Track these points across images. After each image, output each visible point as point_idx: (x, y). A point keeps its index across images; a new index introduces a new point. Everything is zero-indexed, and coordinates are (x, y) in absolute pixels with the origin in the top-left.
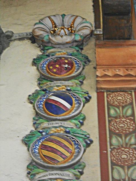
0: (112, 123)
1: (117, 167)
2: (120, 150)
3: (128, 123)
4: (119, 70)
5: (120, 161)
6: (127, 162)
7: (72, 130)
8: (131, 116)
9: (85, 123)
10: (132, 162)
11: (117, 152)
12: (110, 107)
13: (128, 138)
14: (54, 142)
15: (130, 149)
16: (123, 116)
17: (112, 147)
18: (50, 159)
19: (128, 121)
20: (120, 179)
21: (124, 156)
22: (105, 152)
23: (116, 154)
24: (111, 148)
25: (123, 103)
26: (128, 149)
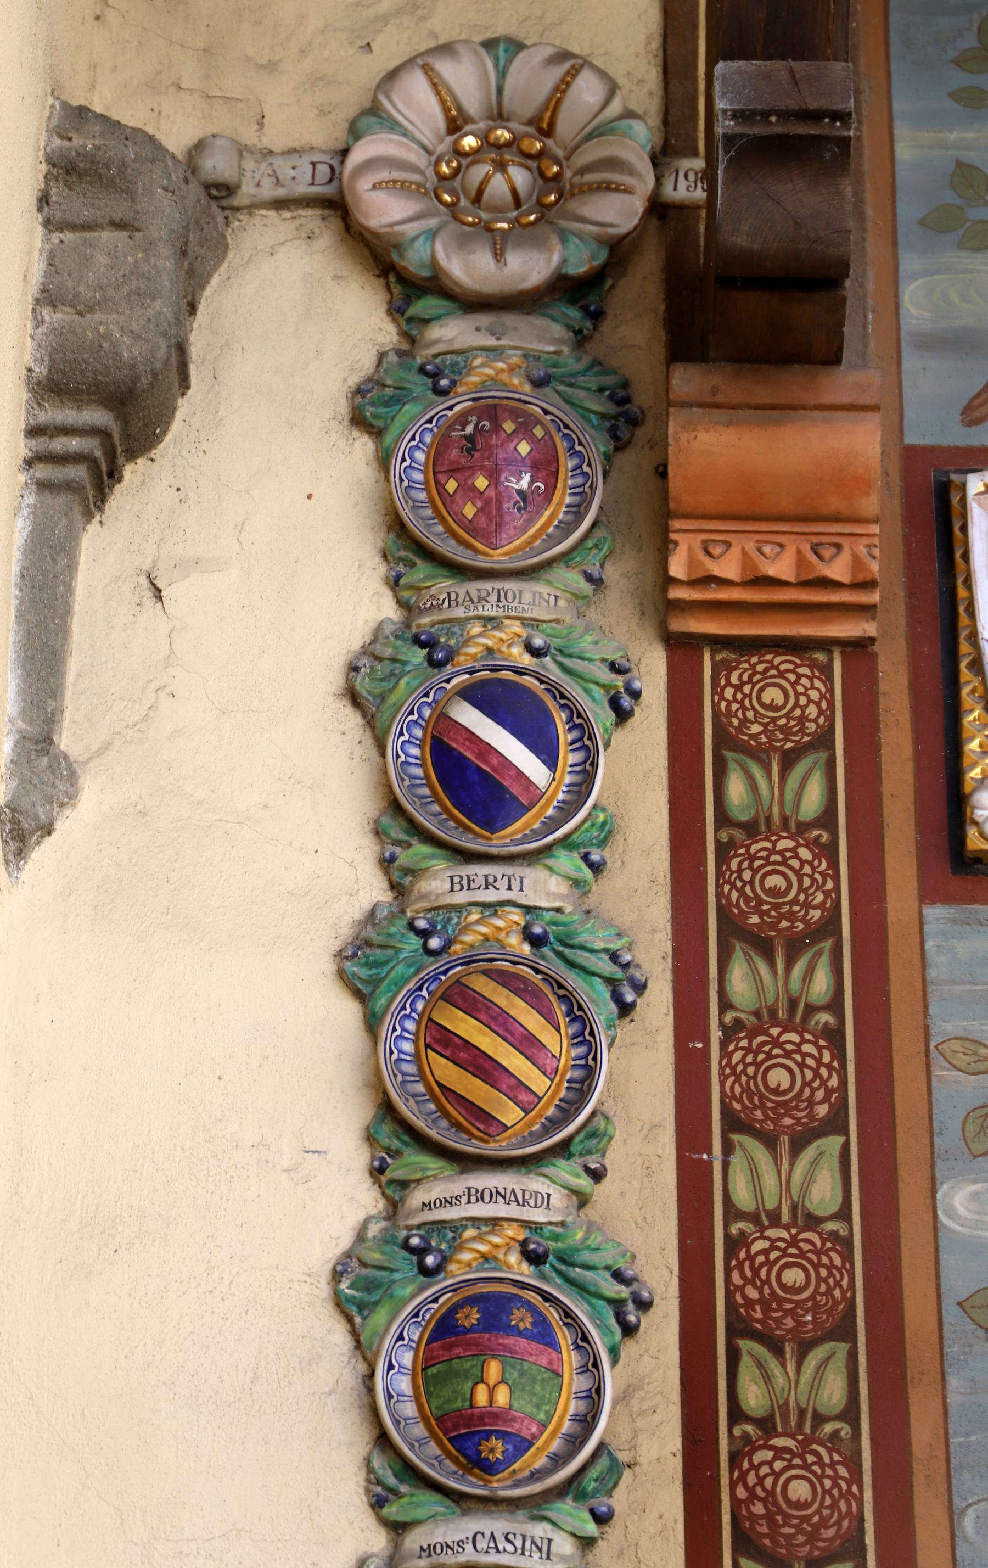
2: (761, 1038)
3: (802, 867)
4: (781, 546)
5: (763, 1107)
6: (785, 1115)
10: (811, 1116)
11: (748, 1050)
12: (728, 754)
13: (799, 968)
14: (482, 1017)
15: (807, 1036)
16: (785, 820)
17: (728, 1018)
18: (467, 1109)
19: (805, 853)
20: (757, 1208)
21: (779, 1078)
22: (700, 1045)
23: (743, 1060)
24: (722, 1024)
25: (785, 730)
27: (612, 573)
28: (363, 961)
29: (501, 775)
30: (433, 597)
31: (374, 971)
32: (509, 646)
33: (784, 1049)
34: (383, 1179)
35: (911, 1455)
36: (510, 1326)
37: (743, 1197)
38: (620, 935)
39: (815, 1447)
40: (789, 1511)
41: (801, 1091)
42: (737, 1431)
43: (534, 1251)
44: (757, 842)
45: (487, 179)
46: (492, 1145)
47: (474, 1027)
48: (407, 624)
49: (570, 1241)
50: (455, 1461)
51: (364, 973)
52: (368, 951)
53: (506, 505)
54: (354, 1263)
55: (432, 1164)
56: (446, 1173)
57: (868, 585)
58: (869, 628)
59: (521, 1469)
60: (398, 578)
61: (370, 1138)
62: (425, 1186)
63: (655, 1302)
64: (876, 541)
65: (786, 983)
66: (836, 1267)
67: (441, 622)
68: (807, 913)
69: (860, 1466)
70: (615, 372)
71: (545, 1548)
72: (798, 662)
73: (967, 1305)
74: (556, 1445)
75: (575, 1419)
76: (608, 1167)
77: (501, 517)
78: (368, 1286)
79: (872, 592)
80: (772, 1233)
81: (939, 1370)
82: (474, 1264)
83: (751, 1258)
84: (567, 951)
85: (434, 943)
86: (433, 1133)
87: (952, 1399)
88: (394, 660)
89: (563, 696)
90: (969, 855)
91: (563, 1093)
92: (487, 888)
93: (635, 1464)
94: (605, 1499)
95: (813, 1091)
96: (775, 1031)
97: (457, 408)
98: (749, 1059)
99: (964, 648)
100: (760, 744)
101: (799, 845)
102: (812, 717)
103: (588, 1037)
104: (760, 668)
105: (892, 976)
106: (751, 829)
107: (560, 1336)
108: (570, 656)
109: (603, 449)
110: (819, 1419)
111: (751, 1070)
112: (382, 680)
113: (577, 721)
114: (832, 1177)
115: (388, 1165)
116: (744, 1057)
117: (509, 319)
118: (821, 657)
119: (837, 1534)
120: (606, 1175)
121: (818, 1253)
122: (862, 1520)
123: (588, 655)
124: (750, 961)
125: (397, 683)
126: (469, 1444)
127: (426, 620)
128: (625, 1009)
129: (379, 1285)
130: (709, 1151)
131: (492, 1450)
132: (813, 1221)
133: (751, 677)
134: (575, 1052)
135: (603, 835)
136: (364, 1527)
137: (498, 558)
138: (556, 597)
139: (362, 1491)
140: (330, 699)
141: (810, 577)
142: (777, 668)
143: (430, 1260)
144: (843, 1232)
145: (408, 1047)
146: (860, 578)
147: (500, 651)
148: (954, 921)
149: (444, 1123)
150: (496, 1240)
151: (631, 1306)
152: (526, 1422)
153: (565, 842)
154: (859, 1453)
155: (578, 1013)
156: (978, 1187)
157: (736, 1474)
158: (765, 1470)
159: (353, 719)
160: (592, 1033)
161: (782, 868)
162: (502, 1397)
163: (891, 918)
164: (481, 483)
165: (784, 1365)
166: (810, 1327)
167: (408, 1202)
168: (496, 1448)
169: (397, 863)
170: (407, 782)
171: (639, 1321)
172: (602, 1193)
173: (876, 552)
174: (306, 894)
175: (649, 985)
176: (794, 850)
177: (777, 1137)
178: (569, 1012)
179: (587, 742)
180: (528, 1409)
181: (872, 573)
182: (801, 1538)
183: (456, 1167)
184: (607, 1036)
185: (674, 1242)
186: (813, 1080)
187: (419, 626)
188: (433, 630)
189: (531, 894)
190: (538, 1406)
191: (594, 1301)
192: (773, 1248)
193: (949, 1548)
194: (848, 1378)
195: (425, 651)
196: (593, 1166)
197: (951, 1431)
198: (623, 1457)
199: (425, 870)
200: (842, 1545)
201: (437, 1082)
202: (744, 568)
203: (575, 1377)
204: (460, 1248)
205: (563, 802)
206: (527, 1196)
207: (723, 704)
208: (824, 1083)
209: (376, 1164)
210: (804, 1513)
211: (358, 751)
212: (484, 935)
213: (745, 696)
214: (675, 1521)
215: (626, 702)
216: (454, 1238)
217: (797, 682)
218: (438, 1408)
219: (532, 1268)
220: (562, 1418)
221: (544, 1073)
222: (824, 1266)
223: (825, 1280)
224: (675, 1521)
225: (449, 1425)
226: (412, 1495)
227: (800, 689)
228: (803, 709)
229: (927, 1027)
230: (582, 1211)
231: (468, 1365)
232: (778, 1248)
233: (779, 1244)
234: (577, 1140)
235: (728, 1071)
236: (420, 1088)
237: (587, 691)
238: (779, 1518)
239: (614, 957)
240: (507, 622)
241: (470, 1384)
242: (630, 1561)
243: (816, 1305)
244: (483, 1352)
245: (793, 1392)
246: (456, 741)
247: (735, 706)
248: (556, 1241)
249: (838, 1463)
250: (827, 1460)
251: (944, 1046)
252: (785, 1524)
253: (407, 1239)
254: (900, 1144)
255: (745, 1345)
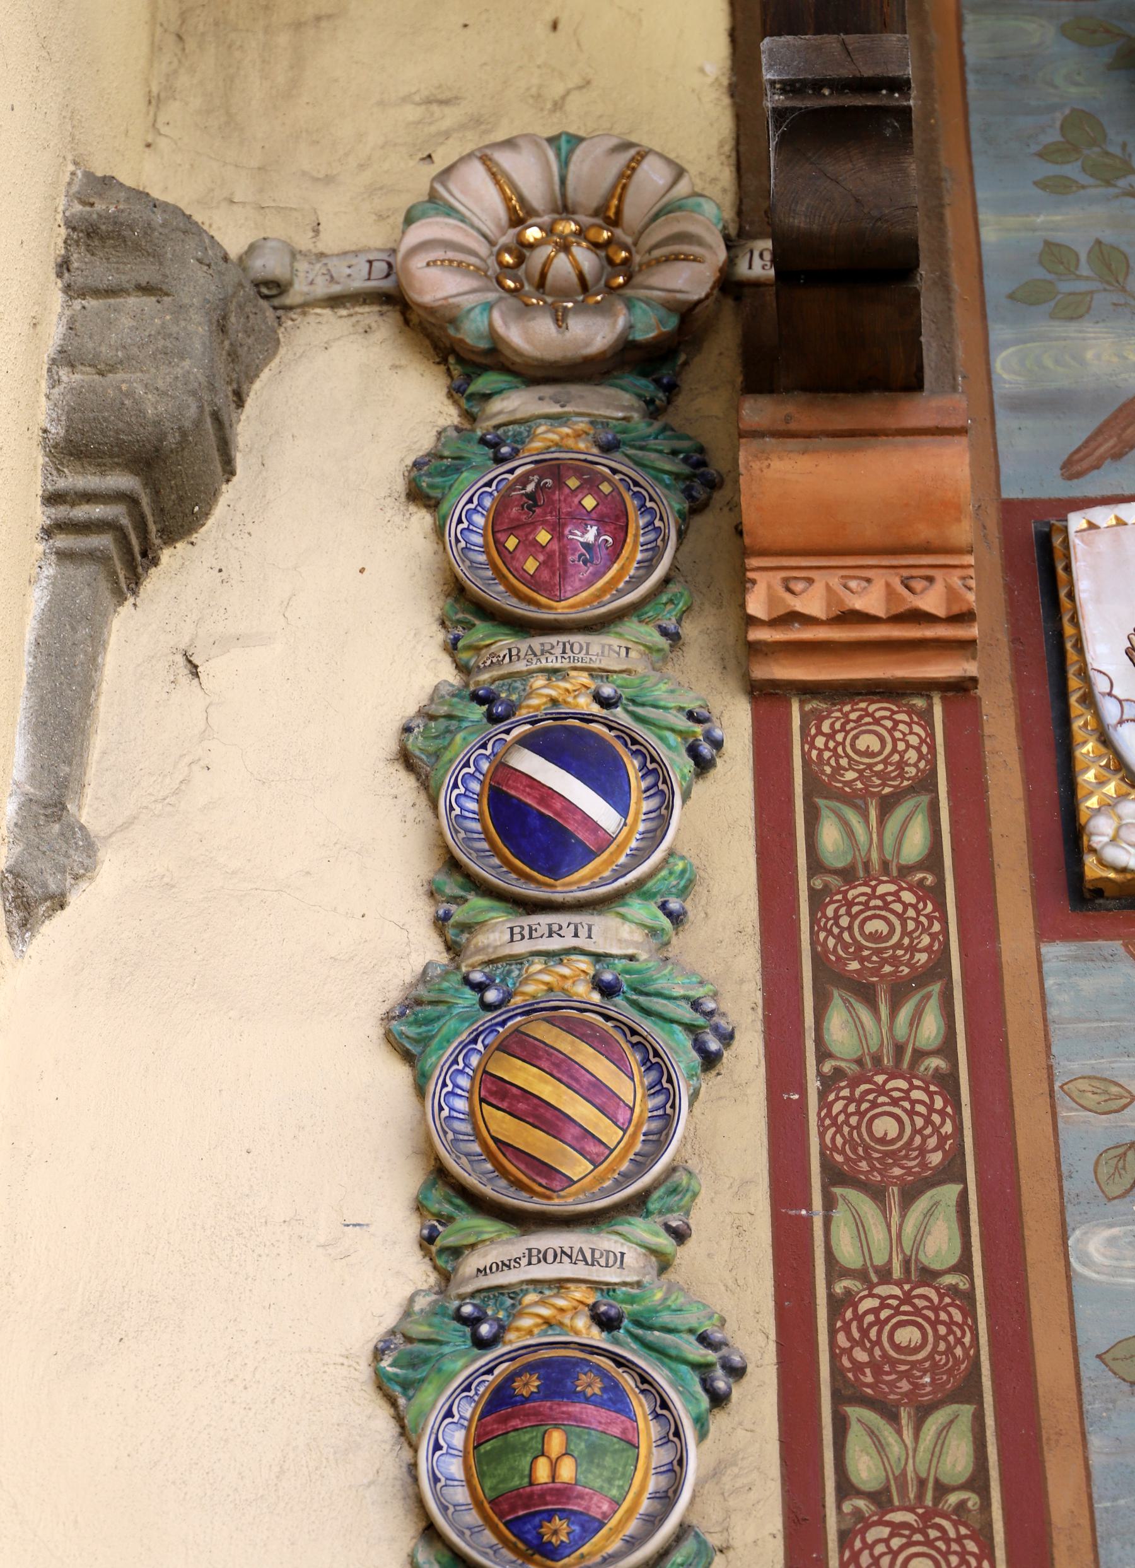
0: (830, 911)
1: (852, 1194)
3: (905, 910)
4: (868, 580)
5: (868, 1157)
6: (894, 1164)
7: (627, 972)
8: (920, 866)
9: (694, 909)
10: (924, 1165)
11: (850, 1100)
12: (821, 802)
13: (905, 1013)
14: (543, 1065)
15: (916, 1082)
16: (885, 865)
17: (827, 1068)
18: (527, 1164)
19: (908, 897)
20: (865, 1265)
21: (885, 1126)
22: (796, 1097)
23: (844, 1110)
24: (819, 1073)
25: (883, 776)
26: (904, 1078)
27: (689, 630)
28: (411, 1019)
29: (565, 820)
30: (493, 655)
31: (424, 1029)
32: (575, 697)
33: (890, 1097)
34: (434, 1249)
35: (1050, 1524)
36: (575, 1392)
37: (848, 1252)
38: (701, 983)
39: (938, 1520)
41: (911, 1139)
42: (847, 1507)
43: (604, 1313)
44: (855, 887)
45: (548, 261)
46: (556, 1201)
47: (534, 1076)
48: (467, 685)
49: (648, 1303)
50: (514, 1549)
51: (412, 1031)
52: (418, 1008)
53: (570, 558)
54: (399, 1340)
55: (488, 1227)
56: (505, 1237)
57: (964, 617)
58: (970, 668)
59: (591, 1554)
60: (457, 639)
61: (420, 1207)
62: (481, 1250)
63: (749, 1370)
64: (971, 572)
65: (891, 1029)
66: (957, 1324)
67: (502, 678)
68: (912, 957)
69: (992, 1539)
70: (689, 438)
72: (895, 708)
73: (1107, 1357)
74: (632, 1527)
75: (655, 1497)
76: (693, 1227)
77: (565, 571)
78: (414, 1362)
79: (970, 627)
80: (882, 1290)
81: (1078, 1429)
82: (536, 1331)
83: (859, 1318)
84: (642, 999)
85: (492, 996)
86: (488, 1190)
87: (1095, 1460)
88: (449, 717)
89: (635, 742)
90: (1088, 886)
91: (638, 1147)
92: (550, 936)
93: (728, 1548)
95: (925, 1139)
96: (880, 1079)
97: (518, 472)
98: (852, 1108)
99: (1074, 683)
100: (855, 790)
101: (901, 889)
102: (912, 761)
103: (666, 1085)
104: (853, 716)
105: (1009, 1016)
106: (848, 875)
107: (635, 1403)
108: (643, 705)
109: (677, 507)
110: (942, 1490)
111: (854, 1120)
112: (436, 737)
113: (651, 766)
114: (949, 1228)
115: (439, 1233)
116: (846, 1106)
117: (575, 389)
118: (920, 703)
120: (690, 1235)
121: (935, 1309)
123: (662, 703)
124: (850, 1008)
125: (452, 739)
126: (529, 1526)
127: (485, 677)
128: (710, 1060)
129: (426, 1360)
130: (808, 1206)
131: (555, 1532)
132: (928, 1276)
133: (843, 726)
134: (651, 1103)
135: (682, 883)
137: (561, 610)
138: (628, 649)
140: (382, 765)
141: (901, 609)
142: (872, 715)
143: (485, 1329)
144: (963, 1284)
145: (461, 1104)
146: (956, 610)
147: (565, 702)
148: (1076, 958)
149: (503, 1183)
150: (561, 1303)
151: (719, 1372)
152: (595, 1499)
153: (637, 887)
154: (989, 1525)
155: (654, 1060)
156: (1115, 1231)
157: (847, 1554)
158: (880, 1549)
159: (406, 783)
160: (670, 1080)
161: (883, 913)
162: (567, 1471)
163: (1006, 957)
164: (543, 537)
165: (899, 1432)
166: (928, 1389)
167: (461, 1271)
168: (560, 1530)
169: (452, 921)
170: (462, 835)
171: (730, 1389)
172: (686, 1255)
173: (972, 583)
174: (352, 959)
175: (737, 1035)
176: (896, 894)
177: (885, 1189)
178: (645, 1061)
179: (661, 786)
180: (598, 1483)
181: (968, 603)
183: (516, 1230)
184: (688, 1086)
185: (769, 1305)
186: (924, 1128)
187: (477, 683)
188: (493, 687)
189: (600, 941)
190: (610, 1481)
191: (674, 1365)
192: (883, 1306)
194: (974, 1443)
195: (485, 708)
196: (674, 1224)
197: (1095, 1496)
198: (714, 1540)
199: (482, 924)
201: (493, 1138)
202: (829, 605)
203: (654, 1450)
204: (521, 1314)
205: (636, 849)
206: (597, 1255)
207: (814, 753)
208: (936, 1130)
209: (426, 1232)
211: (412, 814)
212: (547, 984)
213: (838, 744)
215: (706, 750)
216: (513, 1305)
217: (894, 728)
218: (492, 1489)
219: (604, 1335)
220: (639, 1495)
221: (615, 1123)
222: (943, 1323)
223: (944, 1338)
225: (505, 1507)
227: (898, 735)
228: (902, 754)
229: (1050, 1068)
230: (663, 1276)
231: (527, 1437)
232: (889, 1306)
233: (890, 1301)
234: (655, 1195)
235: (828, 1122)
236: (476, 1148)
237: (662, 739)
239: (696, 1005)
240: (573, 673)
241: (529, 1459)
243: (935, 1365)
244: (544, 1422)
245: (910, 1461)
246: (516, 789)
247: (827, 754)
248: (632, 1304)
249: (966, 1537)
250: (952, 1534)
251: (1070, 1085)
253: (459, 1309)
254: (1024, 1189)
255: (854, 1412)
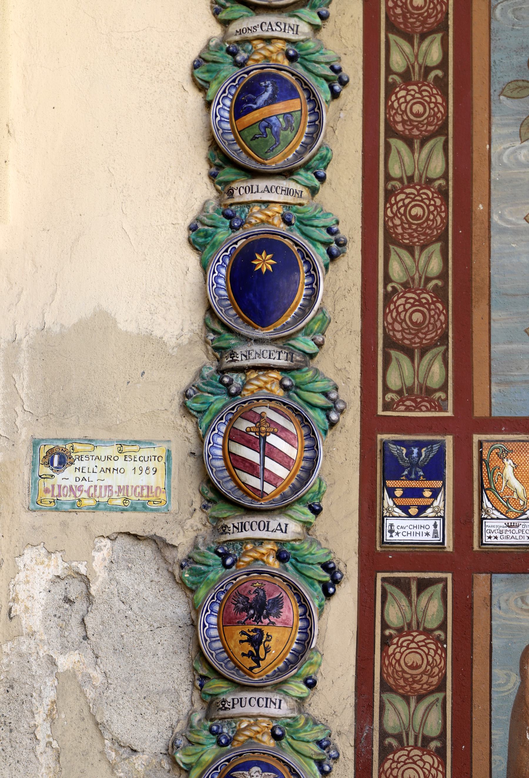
40: (413, 11)
71: (295, 29)
94: (325, 8)
119: (435, 21)
122: (447, 14)
136: (211, 25)
139: (209, 8)
182: (418, 24)
193: (488, 24)
200: (437, 26)
210: (420, 12)
214: (359, 18)
224: (359, 18)
226: (232, 7)
238: (408, 15)
242: (337, 37)
252: (411, 17)
